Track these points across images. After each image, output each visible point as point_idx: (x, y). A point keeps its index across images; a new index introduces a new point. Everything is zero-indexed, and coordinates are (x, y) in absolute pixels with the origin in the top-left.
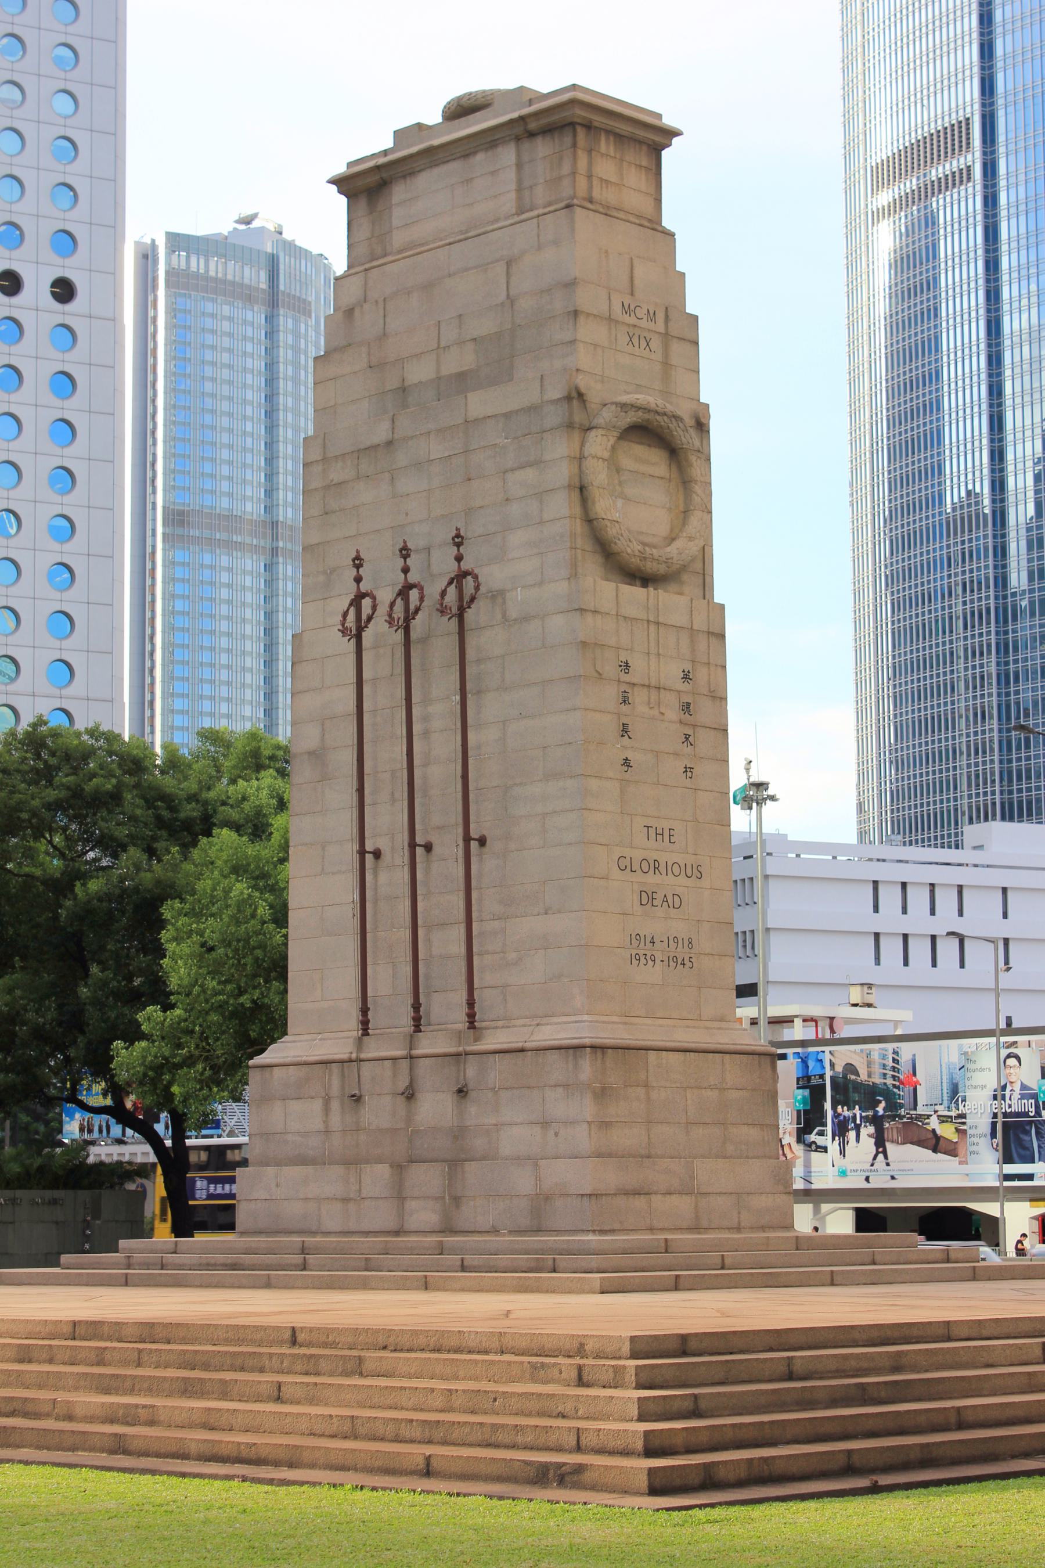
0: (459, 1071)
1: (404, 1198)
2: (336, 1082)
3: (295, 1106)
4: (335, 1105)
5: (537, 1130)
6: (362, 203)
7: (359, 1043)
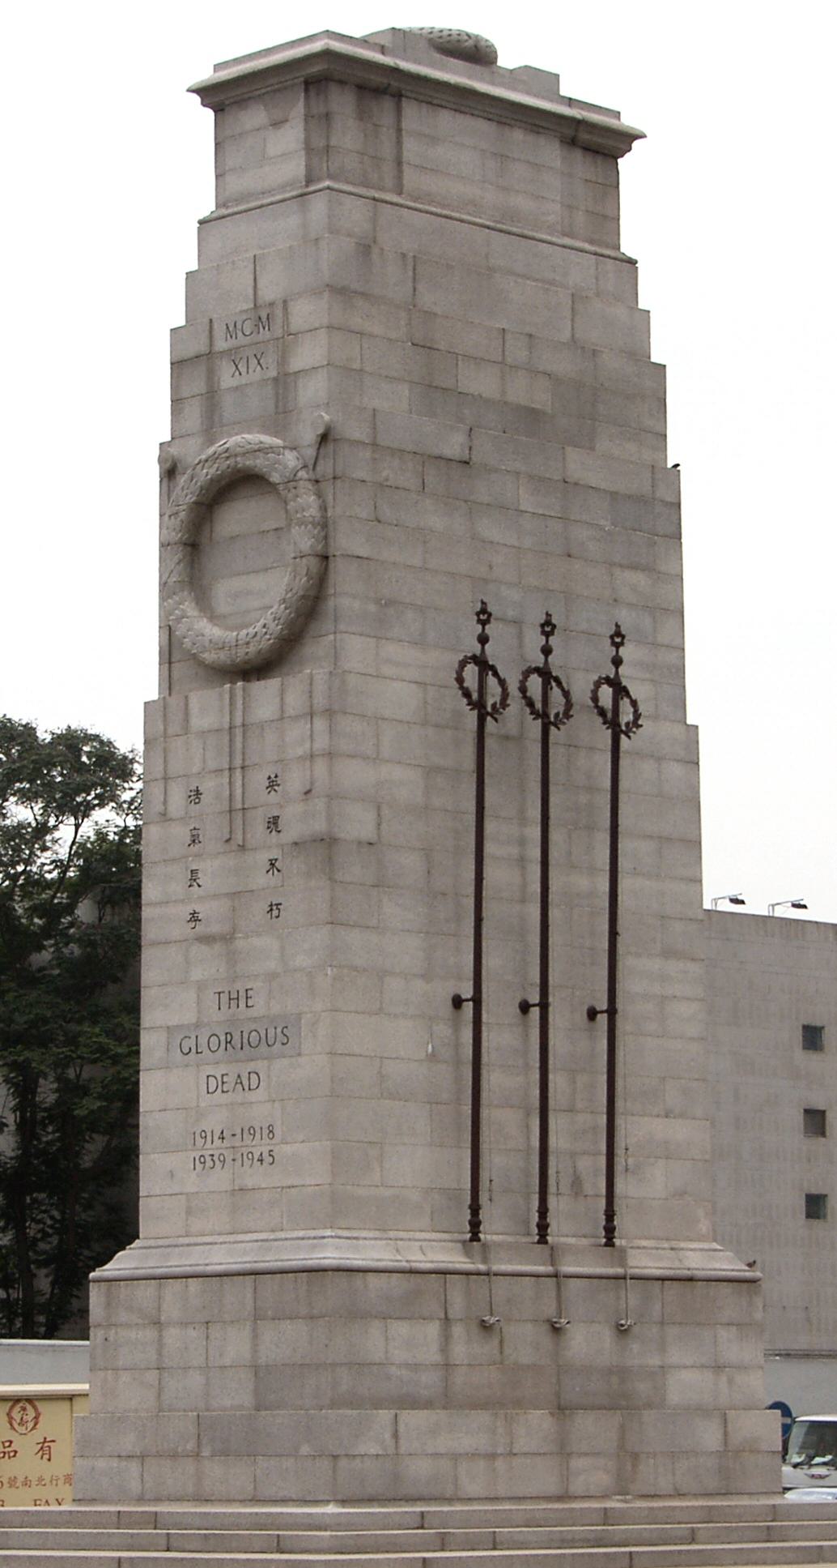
0: (618, 1298)
1: (570, 1455)
3: (401, 1329)
4: (458, 1330)
5: (709, 1375)
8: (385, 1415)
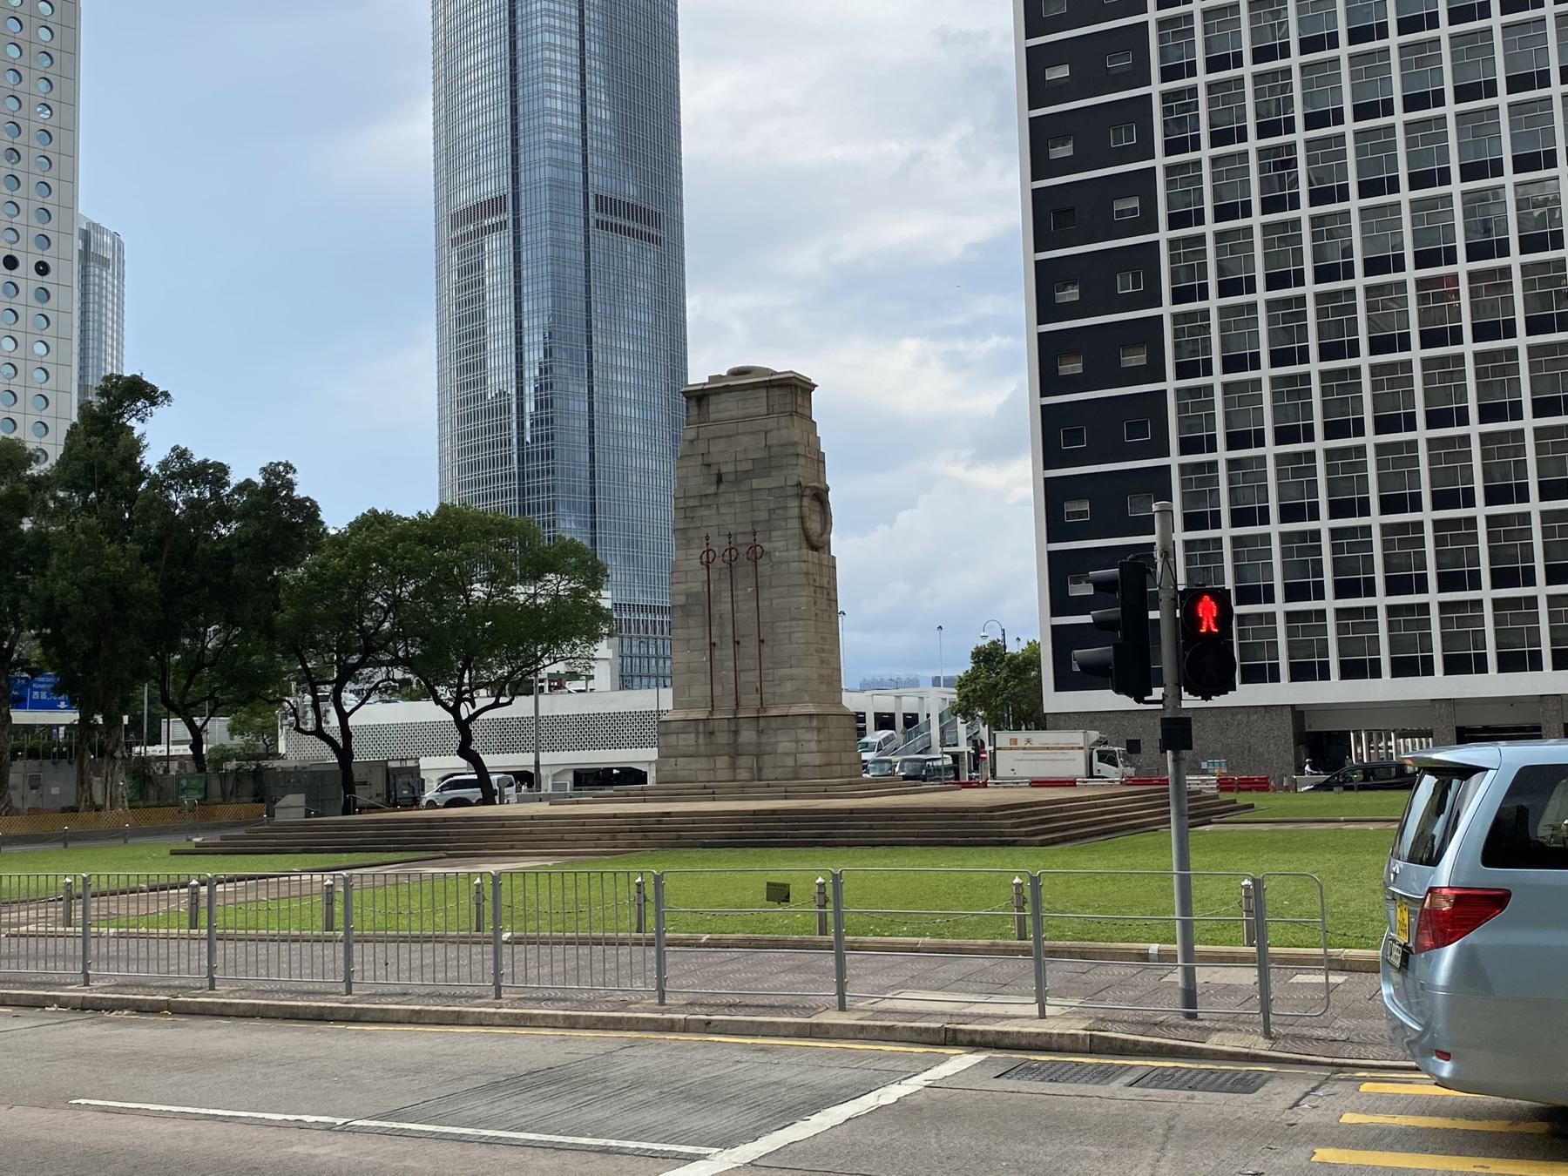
2: (701, 728)
4: (701, 736)
6: (693, 403)
7: (711, 713)
8: (673, 760)
